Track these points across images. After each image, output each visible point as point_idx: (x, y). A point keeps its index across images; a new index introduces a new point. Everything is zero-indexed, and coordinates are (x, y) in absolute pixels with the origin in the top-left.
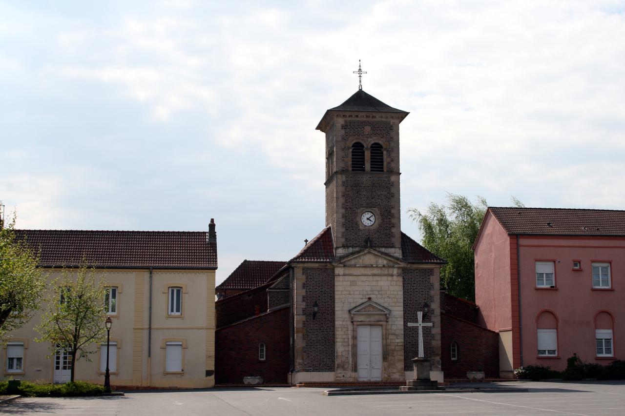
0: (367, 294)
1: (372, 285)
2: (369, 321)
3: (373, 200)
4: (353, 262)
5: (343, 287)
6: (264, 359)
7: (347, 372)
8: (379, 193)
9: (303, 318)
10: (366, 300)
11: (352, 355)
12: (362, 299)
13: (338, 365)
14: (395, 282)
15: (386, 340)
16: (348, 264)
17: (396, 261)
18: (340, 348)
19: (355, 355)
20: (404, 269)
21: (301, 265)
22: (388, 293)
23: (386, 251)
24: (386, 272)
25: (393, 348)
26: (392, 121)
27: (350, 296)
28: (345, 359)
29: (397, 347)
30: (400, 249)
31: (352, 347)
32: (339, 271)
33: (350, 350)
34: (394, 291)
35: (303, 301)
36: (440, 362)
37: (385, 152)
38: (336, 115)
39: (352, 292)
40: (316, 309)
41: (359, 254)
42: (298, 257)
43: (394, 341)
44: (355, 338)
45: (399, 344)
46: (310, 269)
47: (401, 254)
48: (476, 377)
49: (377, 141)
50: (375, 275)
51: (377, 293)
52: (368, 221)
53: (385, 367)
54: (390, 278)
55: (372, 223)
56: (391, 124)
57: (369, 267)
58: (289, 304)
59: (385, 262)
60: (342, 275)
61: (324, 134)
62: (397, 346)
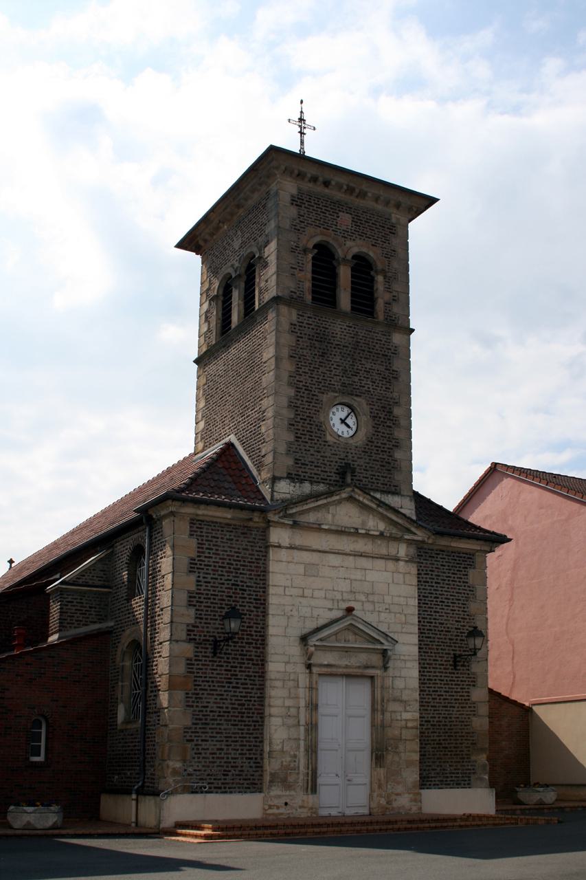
0: (343, 600)
1: (353, 577)
2: (347, 667)
3: (356, 379)
4: (312, 518)
5: (288, 576)
6: (41, 758)
7: (293, 793)
8: (368, 366)
9: (188, 649)
10: (339, 614)
11: (306, 751)
12: (330, 610)
13: (272, 775)
14: (401, 576)
15: (383, 714)
16: (302, 519)
17: (408, 525)
18: (278, 732)
19: (312, 750)
20: (420, 547)
21: (189, 510)
22: (388, 599)
23: (382, 499)
24: (384, 551)
25: (397, 732)
26: (396, 216)
27: (304, 601)
28: (288, 759)
29: (404, 732)
30: (411, 500)
31: (307, 731)
32: (278, 535)
33: (302, 737)
34: (400, 596)
35: (190, 604)
36: (488, 768)
37: (380, 278)
38: (283, 167)
39: (308, 592)
40: (234, 625)
41: (329, 500)
42: (181, 490)
43: (399, 718)
44: (313, 707)
45: (410, 724)
46: (212, 523)
47: (414, 512)
48: (544, 800)
49: (364, 250)
50: (361, 556)
51: (363, 598)
52: (344, 427)
53: (379, 780)
54: (391, 565)
55: (351, 433)
56: (394, 220)
57: (349, 534)
58: (112, 624)
59: (382, 526)
60: (287, 548)
61: (199, 258)
62: (407, 727)
